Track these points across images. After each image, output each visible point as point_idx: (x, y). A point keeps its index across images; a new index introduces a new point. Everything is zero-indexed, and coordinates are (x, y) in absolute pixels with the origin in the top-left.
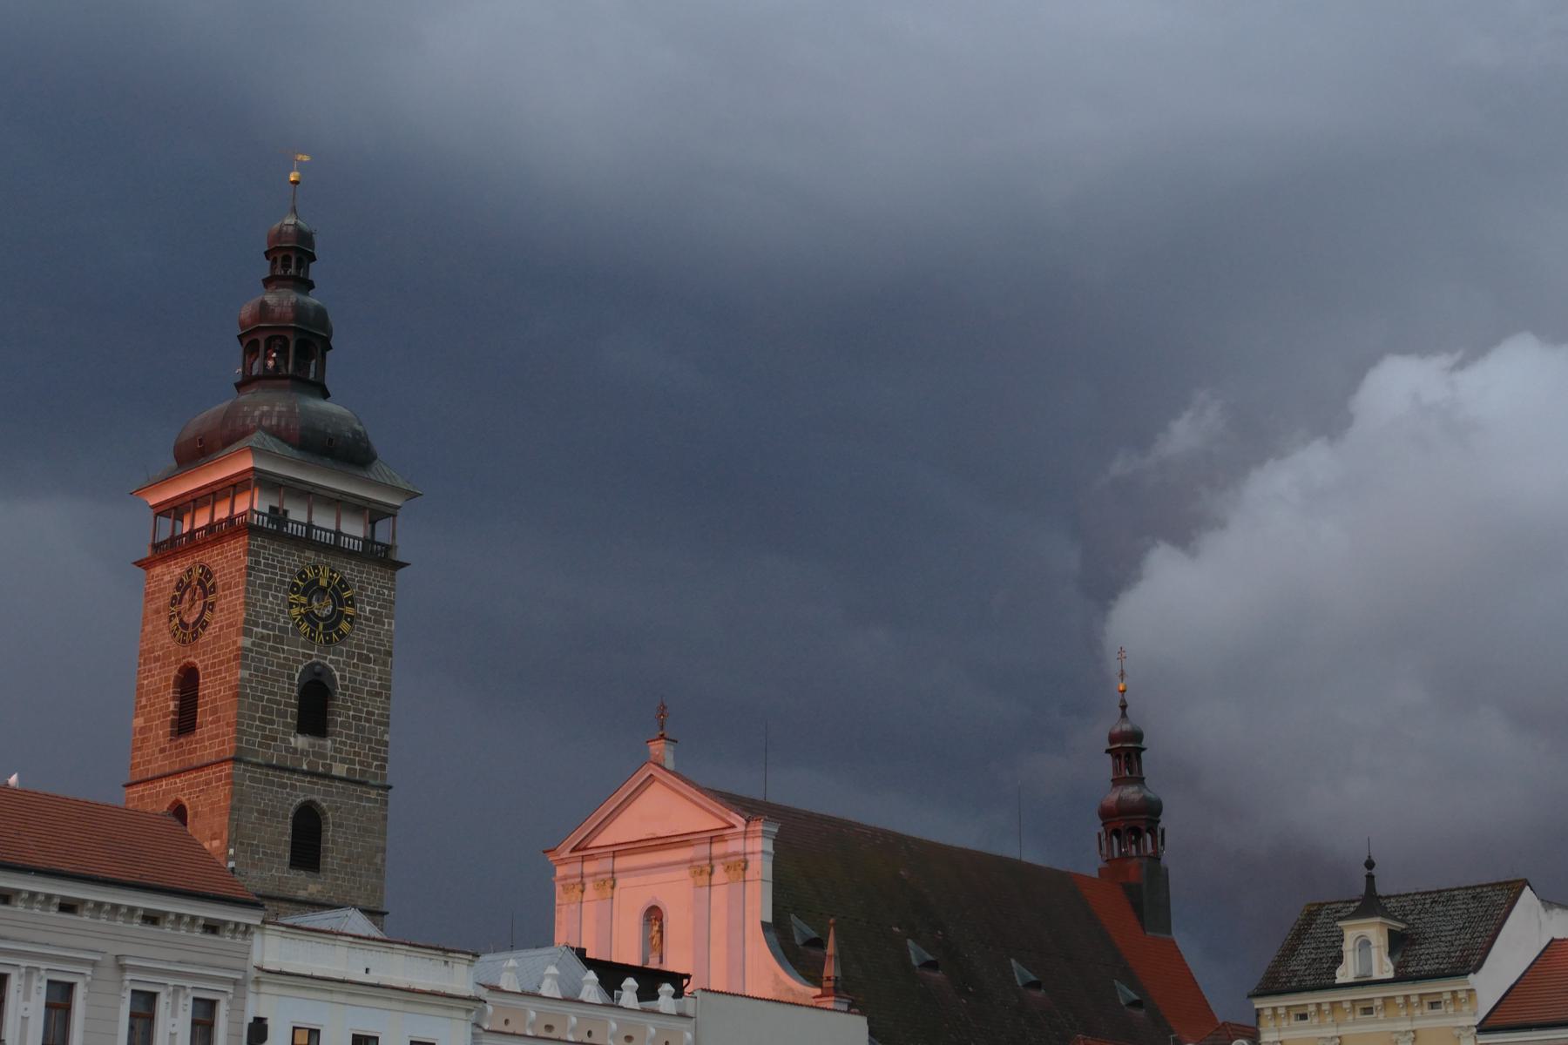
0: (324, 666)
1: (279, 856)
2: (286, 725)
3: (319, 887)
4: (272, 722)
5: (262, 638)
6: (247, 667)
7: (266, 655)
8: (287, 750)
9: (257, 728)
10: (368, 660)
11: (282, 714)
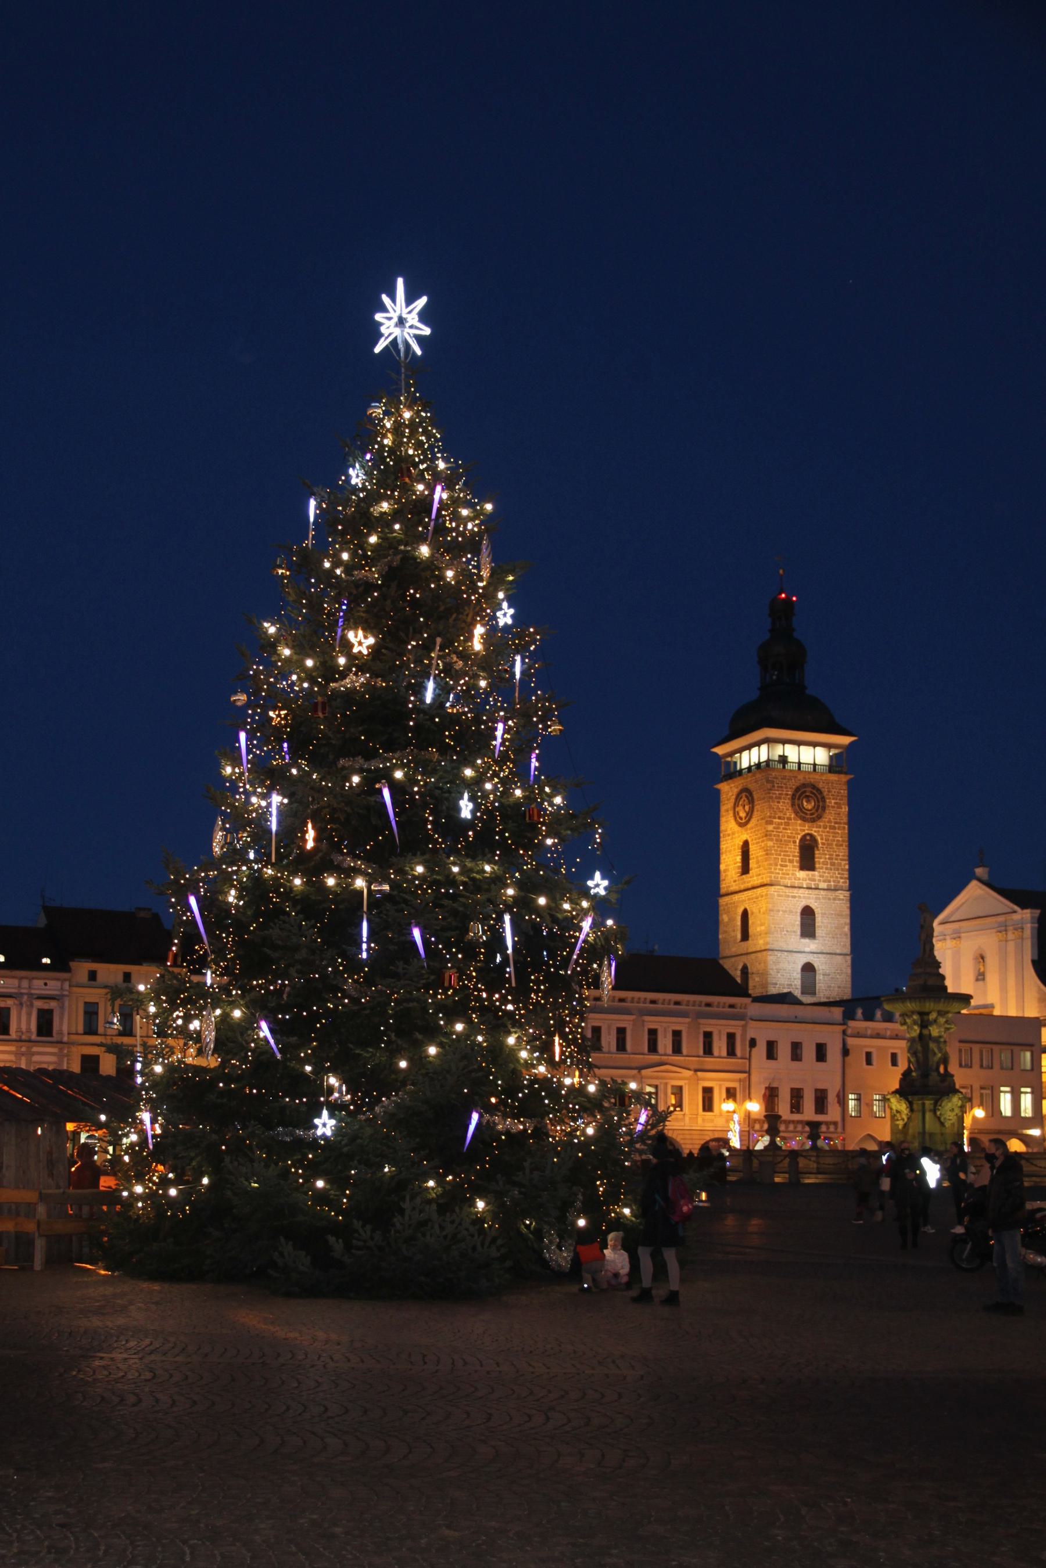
0: (811, 835)
4: (786, 866)
10: (834, 828)
11: (791, 861)
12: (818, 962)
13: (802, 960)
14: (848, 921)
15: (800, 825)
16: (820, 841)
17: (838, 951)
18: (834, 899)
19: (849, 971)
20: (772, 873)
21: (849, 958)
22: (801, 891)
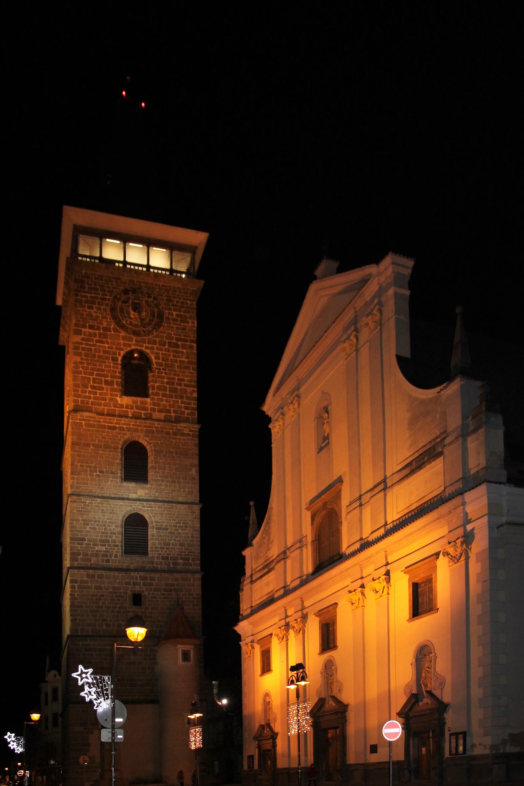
1: (112, 473)
2: (113, 390)
3: (147, 491)
5: (90, 334)
6: (79, 354)
7: (94, 345)
8: (115, 406)
9: (90, 392)
11: (111, 383)
12: (151, 514)
13: (122, 510)
14: (196, 461)
15: (124, 338)
16: (154, 360)
17: (180, 499)
18: (175, 434)
19: (197, 524)
20: (79, 396)
21: (197, 509)
22: (123, 420)
